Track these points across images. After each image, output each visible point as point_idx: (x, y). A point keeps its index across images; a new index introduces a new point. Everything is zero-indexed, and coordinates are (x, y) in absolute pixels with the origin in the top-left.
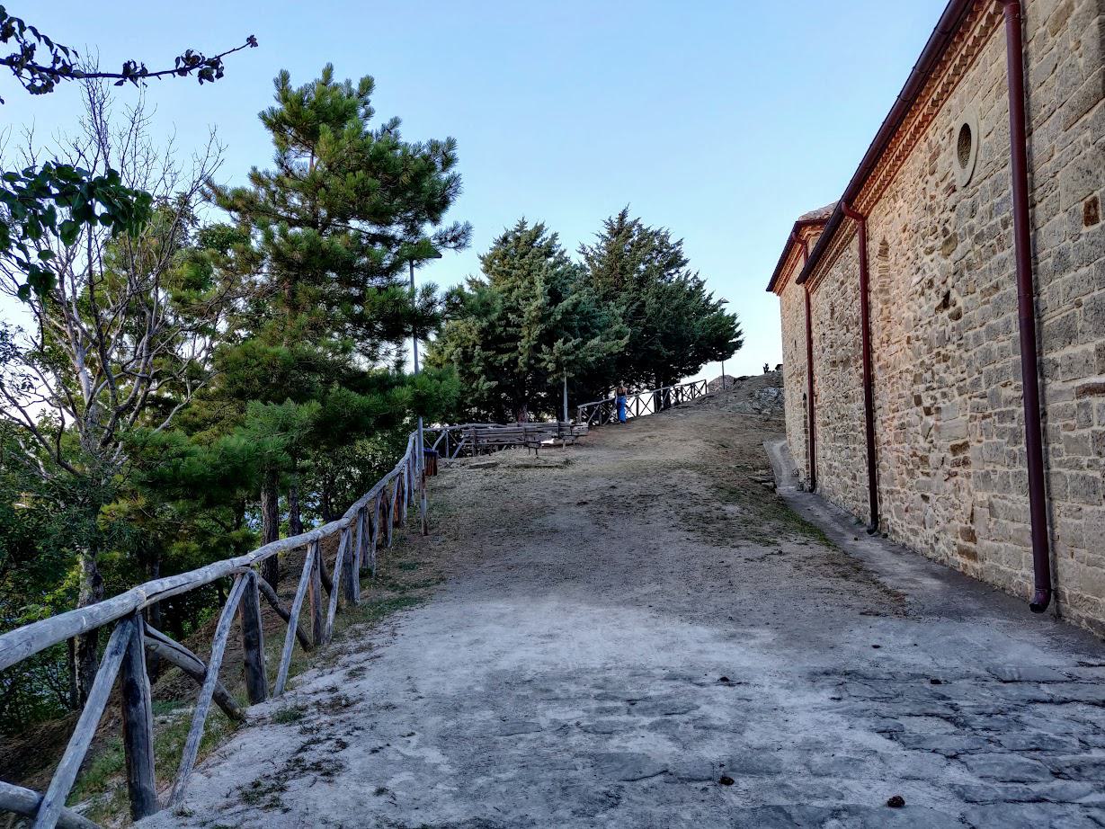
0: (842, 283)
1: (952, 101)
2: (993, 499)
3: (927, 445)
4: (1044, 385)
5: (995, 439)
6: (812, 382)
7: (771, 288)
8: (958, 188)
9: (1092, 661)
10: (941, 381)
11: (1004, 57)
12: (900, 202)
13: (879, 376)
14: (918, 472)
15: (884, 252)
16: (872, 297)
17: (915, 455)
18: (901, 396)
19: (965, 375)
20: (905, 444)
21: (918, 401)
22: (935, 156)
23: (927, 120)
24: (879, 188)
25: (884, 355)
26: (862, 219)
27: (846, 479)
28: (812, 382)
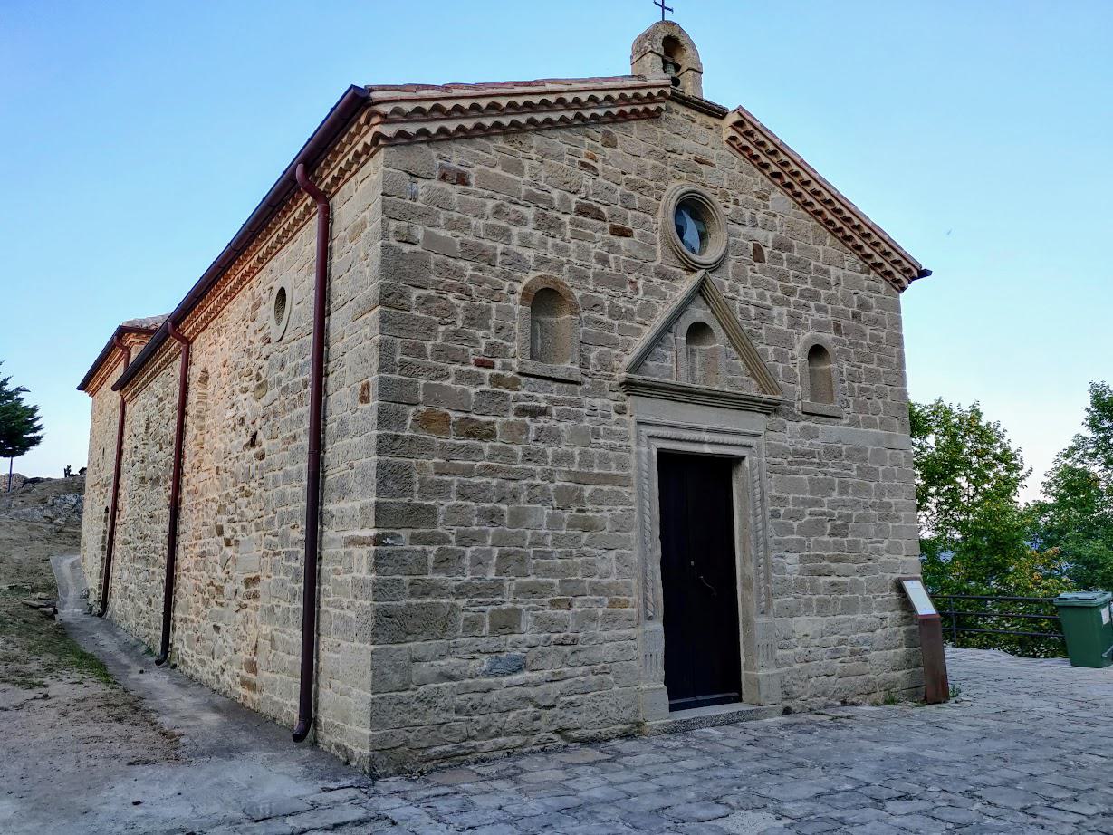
0: (161, 400)
1: (273, 263)
2: (275, 633)
3: (223, 576)
4: (322, 532)
5: (282, 576)
6: (116, 496)
7: (83, 386)
8: (273, 341)
9: (331, 786)
10: (242, 514)
11: (314, 244)
12: (223, 338)
13: (187, 501)
14: (212, 602)
15: (204, 379)
16: (188, 421)
17: (212, 584)
18: (205, 524)
19: (262, 513)
20: (204, 573)
21: (220, 532)
22: (257, 306)
23: (252, 272)
24: (206, 318)
25: (193, 481)
26: (188, 342)
27: (140, 604)
28: (116, 496)
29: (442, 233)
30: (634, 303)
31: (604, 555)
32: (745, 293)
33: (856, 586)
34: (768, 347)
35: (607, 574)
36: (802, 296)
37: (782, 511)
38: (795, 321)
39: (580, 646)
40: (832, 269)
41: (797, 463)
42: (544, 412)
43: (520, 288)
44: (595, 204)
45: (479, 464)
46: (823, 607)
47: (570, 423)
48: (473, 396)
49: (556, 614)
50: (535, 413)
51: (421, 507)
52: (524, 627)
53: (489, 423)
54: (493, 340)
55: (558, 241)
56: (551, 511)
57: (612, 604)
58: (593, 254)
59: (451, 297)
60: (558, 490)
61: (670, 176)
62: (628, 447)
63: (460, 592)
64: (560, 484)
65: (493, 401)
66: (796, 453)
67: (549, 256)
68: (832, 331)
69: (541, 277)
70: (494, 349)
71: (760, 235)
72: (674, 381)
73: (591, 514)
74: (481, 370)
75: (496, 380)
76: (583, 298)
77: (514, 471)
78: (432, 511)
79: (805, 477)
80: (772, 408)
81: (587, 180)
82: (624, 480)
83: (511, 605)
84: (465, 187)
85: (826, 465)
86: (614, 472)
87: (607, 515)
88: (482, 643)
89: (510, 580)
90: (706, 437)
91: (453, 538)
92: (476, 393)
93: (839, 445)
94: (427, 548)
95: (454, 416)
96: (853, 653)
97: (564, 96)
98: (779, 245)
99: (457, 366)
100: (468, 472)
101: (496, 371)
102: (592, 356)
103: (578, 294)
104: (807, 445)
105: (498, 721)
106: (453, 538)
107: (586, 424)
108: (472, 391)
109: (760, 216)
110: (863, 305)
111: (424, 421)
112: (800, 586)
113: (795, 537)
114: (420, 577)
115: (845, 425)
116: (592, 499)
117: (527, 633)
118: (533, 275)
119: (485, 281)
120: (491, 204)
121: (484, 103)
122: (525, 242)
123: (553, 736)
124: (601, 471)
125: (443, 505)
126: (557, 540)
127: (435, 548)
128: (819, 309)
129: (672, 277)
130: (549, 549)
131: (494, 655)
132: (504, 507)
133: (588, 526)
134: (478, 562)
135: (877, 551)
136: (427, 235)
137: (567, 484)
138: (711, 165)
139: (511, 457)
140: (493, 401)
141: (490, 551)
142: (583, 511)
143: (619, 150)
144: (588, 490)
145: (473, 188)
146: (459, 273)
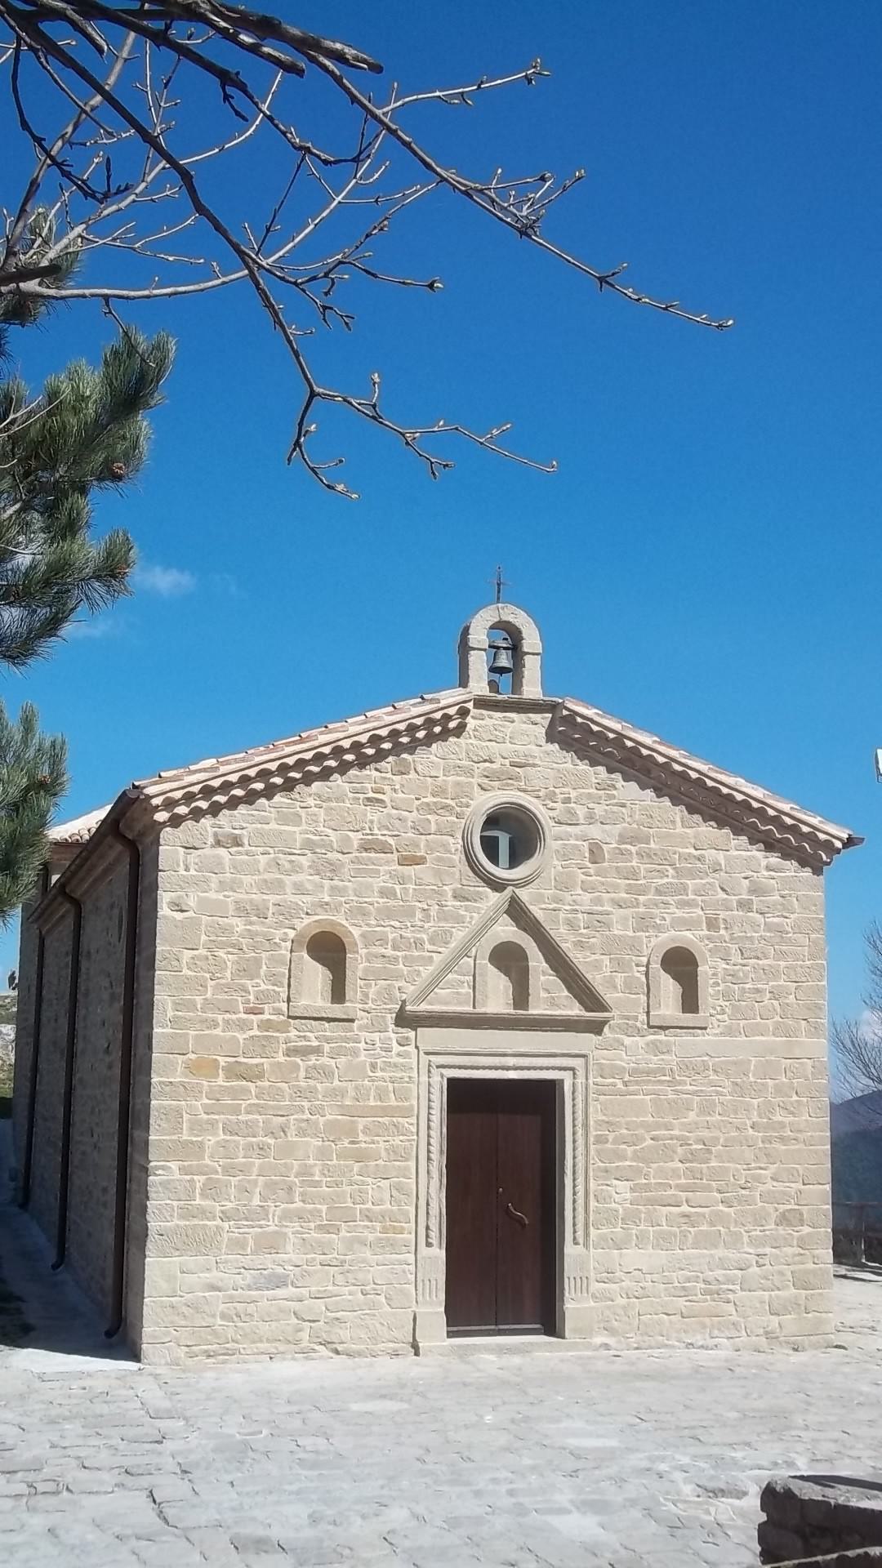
29: (212, 895)
30: (425, 931)
31: (379, 1184)
32: (574, 901)
33: (717, 1219)
34: (603, 957)
35: (381, 1202)
36: (658, 892)
37: (611, 1137)
38: (644, 923)
39: (347, 1267)
40: (710, 854)
41: (637, 1083)
42: (317, 1051)
43: (292, 934)
44: (380, 837)
45: (248, 1102)
46: (663, 1241)
47: (343, 1059)
48: (241, 1041)
49: (324, 1237)
50: (305, 1052)
51: (192, 1142)
52: (289, 1248)
53: (257, 1065)
54: (263, 987)
55: (336, 882)
56: (320, 1143)
57: (385, 1230)
58: (376, 889)
59: (221, 953)
60: (328, 1123)
61: (476, 788)
62: (410, 1077)
63: (225, 1217)
64: (329, 1117)
65: (262, 1045)
66: (634, 1072)
67: (327, 899)
68: (704, 928)
69: (316, 921)
70: (264, 997)
71: (595, 832)
72: (469, 1009)
73: (363, 1145)
74: (252, 1017)
75: (266, 1025)
76: (363, 935)
77: (279, 1108)
78: (201, 1145)
79: (649, 1097)
80: (596, 1028)
81: (373, 814)
82: (406, 1113)
83: (273, 1228)
84: (240, 848)
85: (680, 1083)
86: (393, 1103)
87: (382, 1145)
88: (246, 1261)
89: (276, 1206)
90: (511, 1061)
91: (219, 1169)
92: (245, 1039)
93: (705, 1058)
94: (195, 1177)
95: (222, 1061)
96: (706, 1292)
97: (340, 743)
98: (623, 839)
99: (227, 1016)
100: (236, 1110)
101: (266, 1016)
102: (372, 992)
103: (356, 932)
104: (655, 1061)
105: (264, 1329)
106: (219, 1169)
107: (363, 1058)
108: (241, 1036)
109: (599, 810)
110: (756, 890)
111: (193, 1069)
112: (631, 1217)
113: (628, 1163)
114: (189, 1202)
115: (716, 1035)
116: (366, 1130)
117: (291, 1253)
118: (307, 920)
119: (257, 934)
120: (263, 859)
121: (252, 773)
122: (300, 889)
123: (316, 1347)
124: (379, 1103)
125: (211, 1141)
126: (326, 1171)
127: (203, 1178)
128: (682, 904)
129: (478, 897)
130: (317, 1178)
131: (259, 1272)
132: (271, 1141)
133: (361, 1157)
134: (245, 1190)
135: (758, 1179)
136: (201, 901)
137: (340, 1117)
138: (534, 765)
139: (280, 1093)
140: (262, 1045)
141: (256, 1182)
142: (357, 1143)
143: (413, 775)
144: (361, 1123)
145: (247, 847)
146: (226, 930)
